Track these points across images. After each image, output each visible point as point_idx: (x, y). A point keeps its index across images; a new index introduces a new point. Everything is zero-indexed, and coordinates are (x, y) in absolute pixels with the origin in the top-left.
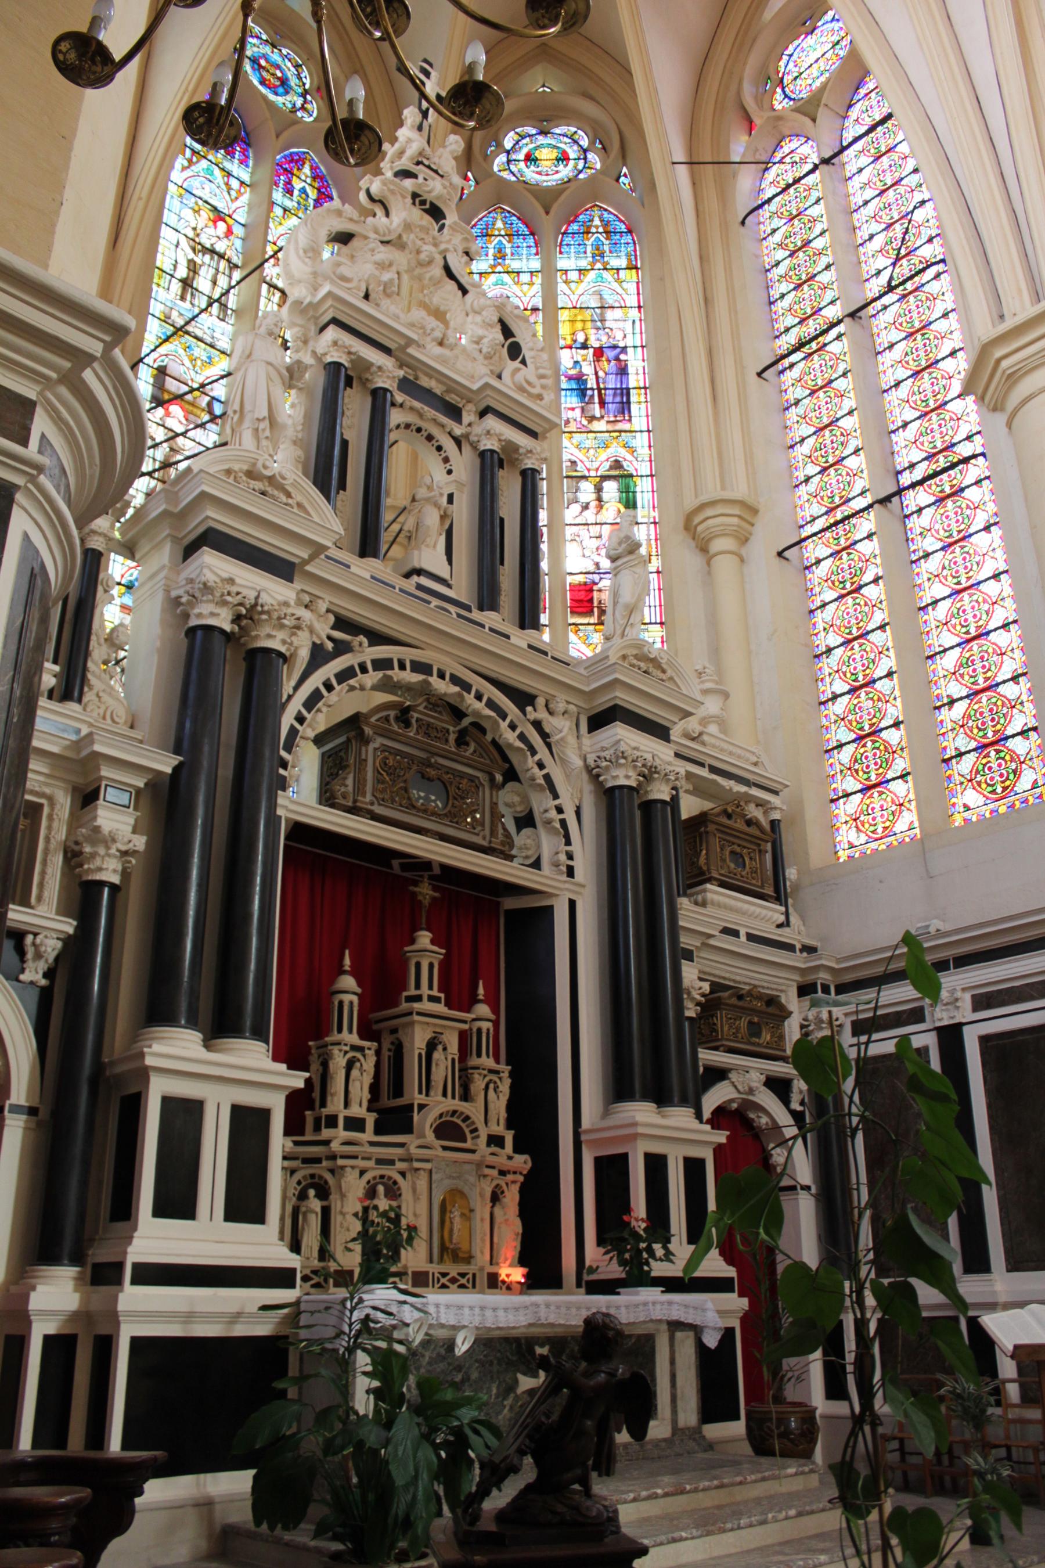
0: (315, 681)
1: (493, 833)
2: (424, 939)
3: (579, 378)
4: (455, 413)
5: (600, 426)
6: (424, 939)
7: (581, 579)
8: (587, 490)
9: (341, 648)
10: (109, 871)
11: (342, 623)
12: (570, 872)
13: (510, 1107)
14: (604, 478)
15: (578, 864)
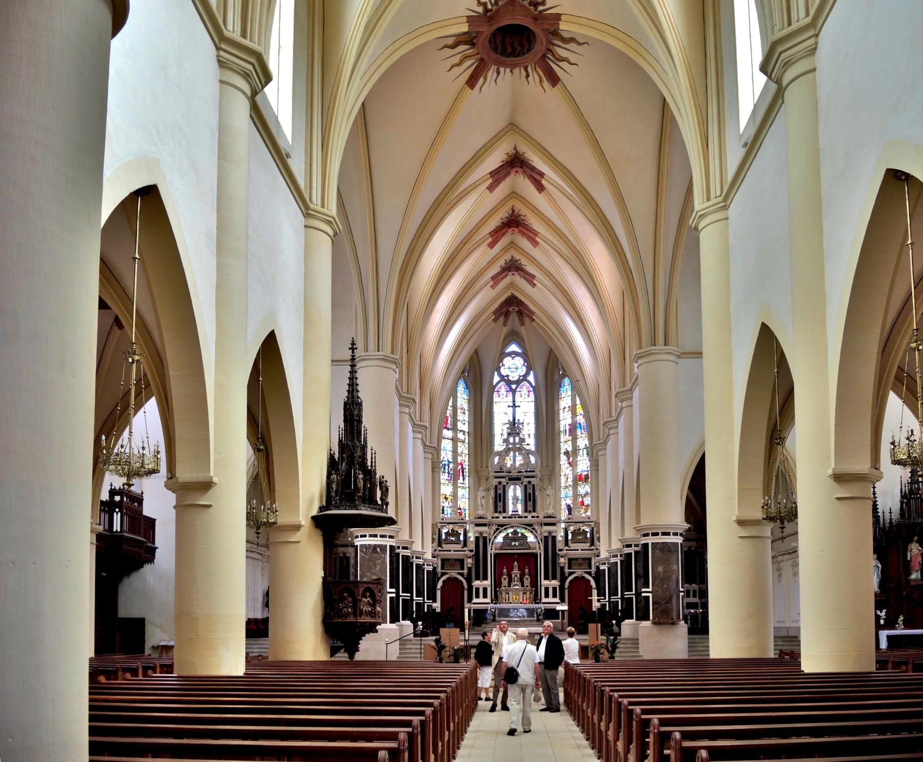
0: (495, 534)
1: (526, 545)
2: (516, 563)
3: (580, 424)
4: (518, 479)
5: (583, 435)
6: (516, 563)
7: (580, 473)
8: (581, 451)
9: (499, 529)
10: (470, 566)
11: (499, 525)
12: (540, 549)
13: (530, 582)
14: (584, 449)
15: (541, 547)
